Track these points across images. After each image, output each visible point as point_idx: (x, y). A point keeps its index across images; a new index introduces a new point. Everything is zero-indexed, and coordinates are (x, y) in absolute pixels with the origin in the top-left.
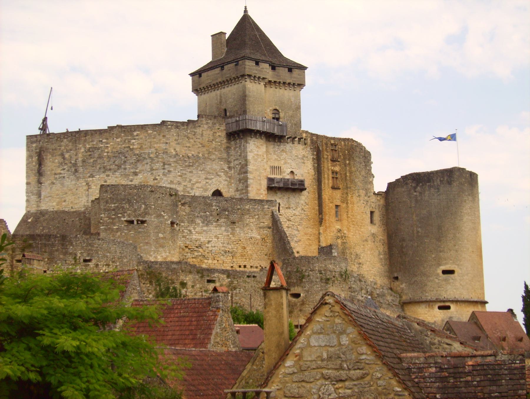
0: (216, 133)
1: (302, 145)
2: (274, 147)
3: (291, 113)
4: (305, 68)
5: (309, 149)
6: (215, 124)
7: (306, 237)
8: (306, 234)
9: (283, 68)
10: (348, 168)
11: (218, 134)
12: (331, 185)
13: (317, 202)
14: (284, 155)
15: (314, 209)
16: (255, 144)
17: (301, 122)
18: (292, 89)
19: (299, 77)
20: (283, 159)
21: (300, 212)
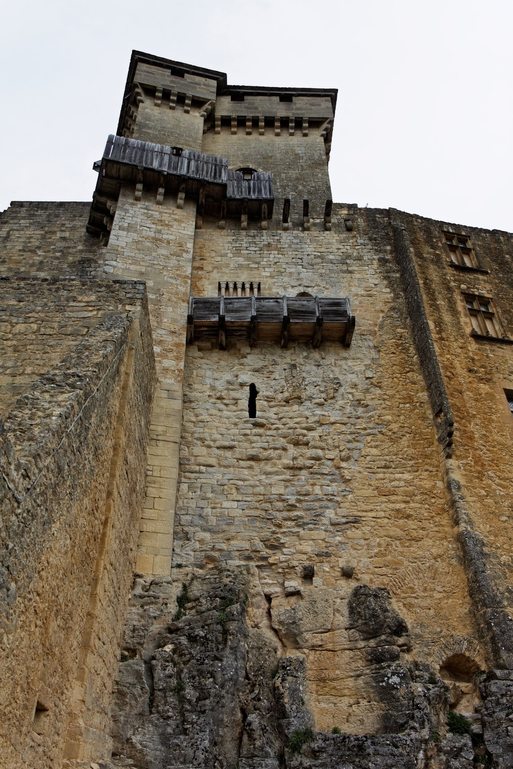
0: (54, 233)
3: (293, 173)
4: (331, 95)
6: (57, 216)
8: (385, 493)
9: (267, 98)
11: (59, 235)
13: (418, 377)
14: (274, 255)
17: (329, 188)
18: (299, 133)
19: (313, 108)
20: (270, 266)
21: (348, 409)
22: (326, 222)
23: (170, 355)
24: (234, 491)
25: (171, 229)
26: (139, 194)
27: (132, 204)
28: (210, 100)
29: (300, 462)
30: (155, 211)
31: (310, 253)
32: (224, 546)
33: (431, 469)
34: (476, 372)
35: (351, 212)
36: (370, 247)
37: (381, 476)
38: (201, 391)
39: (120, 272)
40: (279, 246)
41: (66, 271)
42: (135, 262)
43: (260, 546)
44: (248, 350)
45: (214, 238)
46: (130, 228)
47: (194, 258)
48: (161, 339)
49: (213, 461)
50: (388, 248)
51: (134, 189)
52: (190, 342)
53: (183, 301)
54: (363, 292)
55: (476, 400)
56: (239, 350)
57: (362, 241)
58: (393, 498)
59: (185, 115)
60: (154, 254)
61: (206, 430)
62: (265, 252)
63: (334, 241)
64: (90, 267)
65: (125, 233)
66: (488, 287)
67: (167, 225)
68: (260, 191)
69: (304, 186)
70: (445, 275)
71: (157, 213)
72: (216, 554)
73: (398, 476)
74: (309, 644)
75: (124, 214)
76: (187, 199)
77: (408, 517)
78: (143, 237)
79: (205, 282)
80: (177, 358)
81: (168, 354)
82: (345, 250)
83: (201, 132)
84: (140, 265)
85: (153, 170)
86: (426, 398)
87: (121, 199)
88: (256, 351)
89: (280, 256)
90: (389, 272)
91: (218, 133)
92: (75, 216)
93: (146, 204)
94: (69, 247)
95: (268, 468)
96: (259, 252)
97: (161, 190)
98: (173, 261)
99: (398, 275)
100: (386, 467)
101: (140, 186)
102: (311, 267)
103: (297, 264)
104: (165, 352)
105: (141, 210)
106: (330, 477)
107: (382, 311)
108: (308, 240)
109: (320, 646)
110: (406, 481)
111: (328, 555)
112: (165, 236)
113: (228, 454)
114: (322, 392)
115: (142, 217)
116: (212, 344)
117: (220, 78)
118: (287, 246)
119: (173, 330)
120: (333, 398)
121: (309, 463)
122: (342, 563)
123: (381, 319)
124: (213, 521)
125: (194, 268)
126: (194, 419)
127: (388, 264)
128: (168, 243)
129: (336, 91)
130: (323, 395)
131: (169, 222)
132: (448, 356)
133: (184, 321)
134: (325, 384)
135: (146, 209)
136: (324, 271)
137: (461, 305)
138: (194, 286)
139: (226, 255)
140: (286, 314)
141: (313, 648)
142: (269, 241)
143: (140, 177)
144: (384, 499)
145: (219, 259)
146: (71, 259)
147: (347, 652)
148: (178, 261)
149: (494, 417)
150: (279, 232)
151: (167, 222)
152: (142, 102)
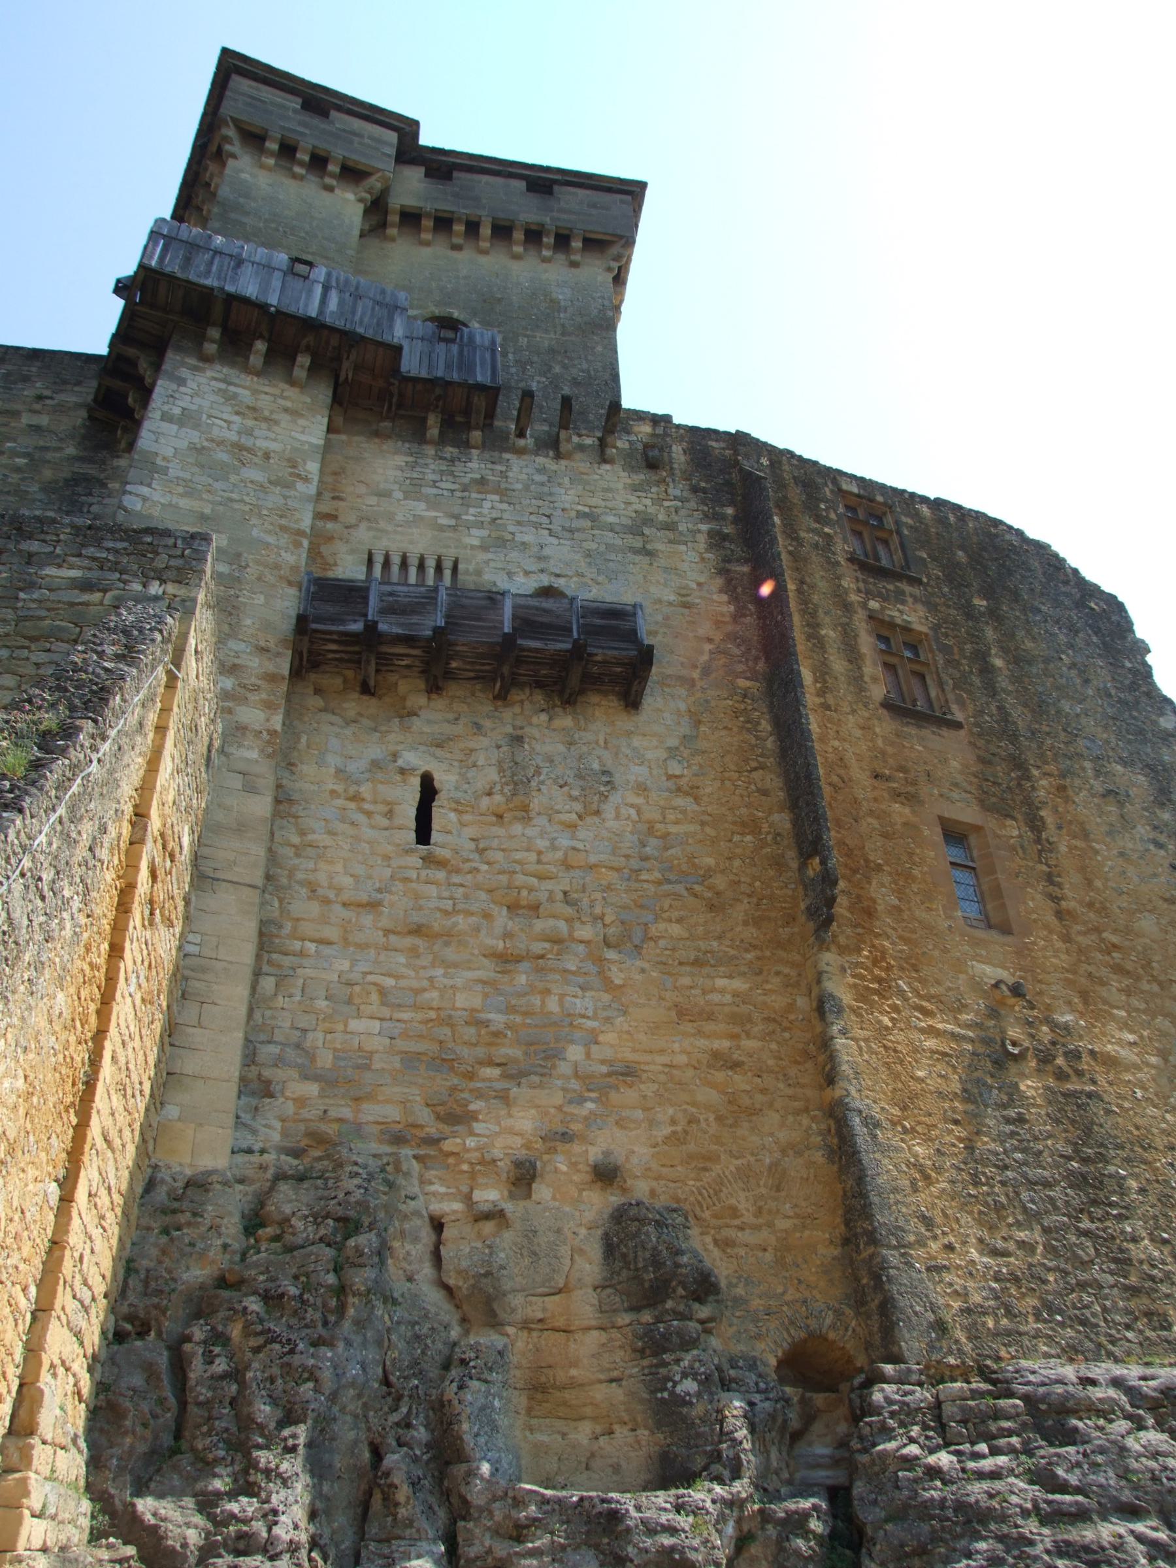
1: (631, 468)
2: (412, 466)
3: (545, 339)
4: (633, 192)
5: (677, 489)
6: (26, 379)
7: (683, 1047)
10: (990, 633)
11: (26, 419)
12: (878, 692)
13: (773, 781)
14: (490, 505)
15: (751, 826)
16: (231, 398)
17: (615, 377)
19: (594, 211)
22: (602, 444)
23: (253, 697)
24: (375, 997)
25: (276, 428)
26: (211, 348)
27: (195, 369)
28: (379, 170)
29: (521, 944)
30: (244, 388)
31: (567, 506)
32: (347, 1113)
33: (786, 970)
34: (888, 779)
35: (660, 431)
36: (693, 504)
37: (686, 981)
38: (314, 779)
39: (156, 512)
40: (503, 486)
41: (34, 500)
42: (190, 493)
43: (424, 1116)
44: (422, 700)
45: (366, 455)
46: (186, 419)
47: (319, 494)
48: (237, 661)
49: (331, 933)
50: (730, 511)
51: (200, 338)
52: (297, 673)
53: (290, 583)
54: (672, 598)
55: (886, 836)
56: (404, 699)
57: (678, 493)
58: (709, 1027)
59: (325, 194)
60: (233, 478)
61: (322, 865)
62: (474, 495)
63: (620, 486)
64: (90, 494)
65: (175, 427)
66: (921, 610)
67: (266, 419)
68: (471, 369)
69: (565, 367)
70: (839, 578)
71: (247, 392)
72: (331, 1129)
73: (720, 982)
74: (518, 1316)
75: (175, 387)
76: (314, 370)
77: (736, 1065)
78: (213, 440)
79: (341, 548)
80: (269, 706)
81: (249, 695)
82: (640, 507)
83: (357, 232)
84: (202, 499)
85: (246, 301)
86: (788, 826)
87: (170, 355)
88: (439, 703)
89: (505, 506)
90: (729, 561)
91: (393, 240)
92: (65, 382)
93: (225, 370)
94: (46, 449)
95: (450, 954)
96: (458, 494)
97: (260, 346)
98: (274, 498)
99: (746, 569)
100: (697, 963)
101: (215, 333)
102: (568, 535)
103: (537, 526)
104: (242, 691)
105: (213, 383)
106: (581, 980)
107: (710, 640)
108: (566, 480)
109: (540, 1321)
110: (735, 994)
111: (566, 1137)
112: (259, 443)
113: (367, 920)
114: (576, 799)
115: (213, 398)
116: (345, 681)
117: (407, 128)
118: (519, 486)
119: (262, 644)
120: (597, 813)
121: (538, 947)
122: (594, 1154)
123: (706, 657)
124: (325, 1060)
125: (319, 516)
126: (296, 840)
127: (727, 544)
128: (267, 456)
129: (643, 186)
130: (578, 807)
131: (272, 412)
132: (836, 743)
133: (287, 626)
134: (581, 783)
135: (224, 381)
136: (594, 546)
137: (866, 643)
138: (314, 554)
139: (386, 494)
140: (507, 629)
141: (526, 1325)
142: (484, 472)
143: (218, 310)
144: (689, 1027)
145: (373, 500)
146: (48, 474)
147: (595, 1333)
148: (285, 497)
149: (915, 872)
150: (506, 456)
151: (267, 413)
152: (234, 156)
